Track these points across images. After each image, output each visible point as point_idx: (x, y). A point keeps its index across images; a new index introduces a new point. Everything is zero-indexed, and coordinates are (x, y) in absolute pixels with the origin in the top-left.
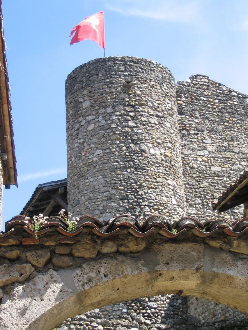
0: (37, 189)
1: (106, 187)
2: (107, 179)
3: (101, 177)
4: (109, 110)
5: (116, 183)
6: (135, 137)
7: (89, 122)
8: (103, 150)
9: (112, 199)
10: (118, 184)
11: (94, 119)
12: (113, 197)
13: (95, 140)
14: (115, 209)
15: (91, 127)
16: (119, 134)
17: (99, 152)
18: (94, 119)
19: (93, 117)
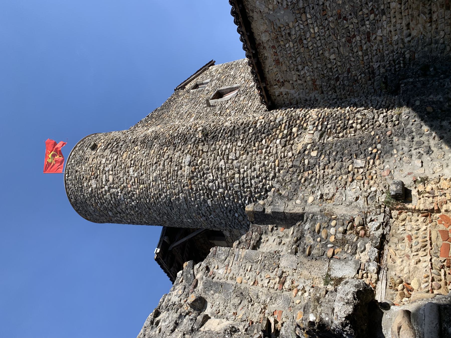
0: (157, 260)
1: (160, 164)
2: (154, 162)
3: (151, 168)
4: (104, 160)
5: (160, 155)
6: (132, 141)
7: (107, 181)
8: (130, 167)
9: (171, 158)
10: (162, 152)
11: (106, 176)
12: (170, 157)
13: (121, 175)
14: (181, 154)
15: (111, 178)
16: (124, 153)
17: (131, 170)
18: (106, 176)
19: (105, 175)
